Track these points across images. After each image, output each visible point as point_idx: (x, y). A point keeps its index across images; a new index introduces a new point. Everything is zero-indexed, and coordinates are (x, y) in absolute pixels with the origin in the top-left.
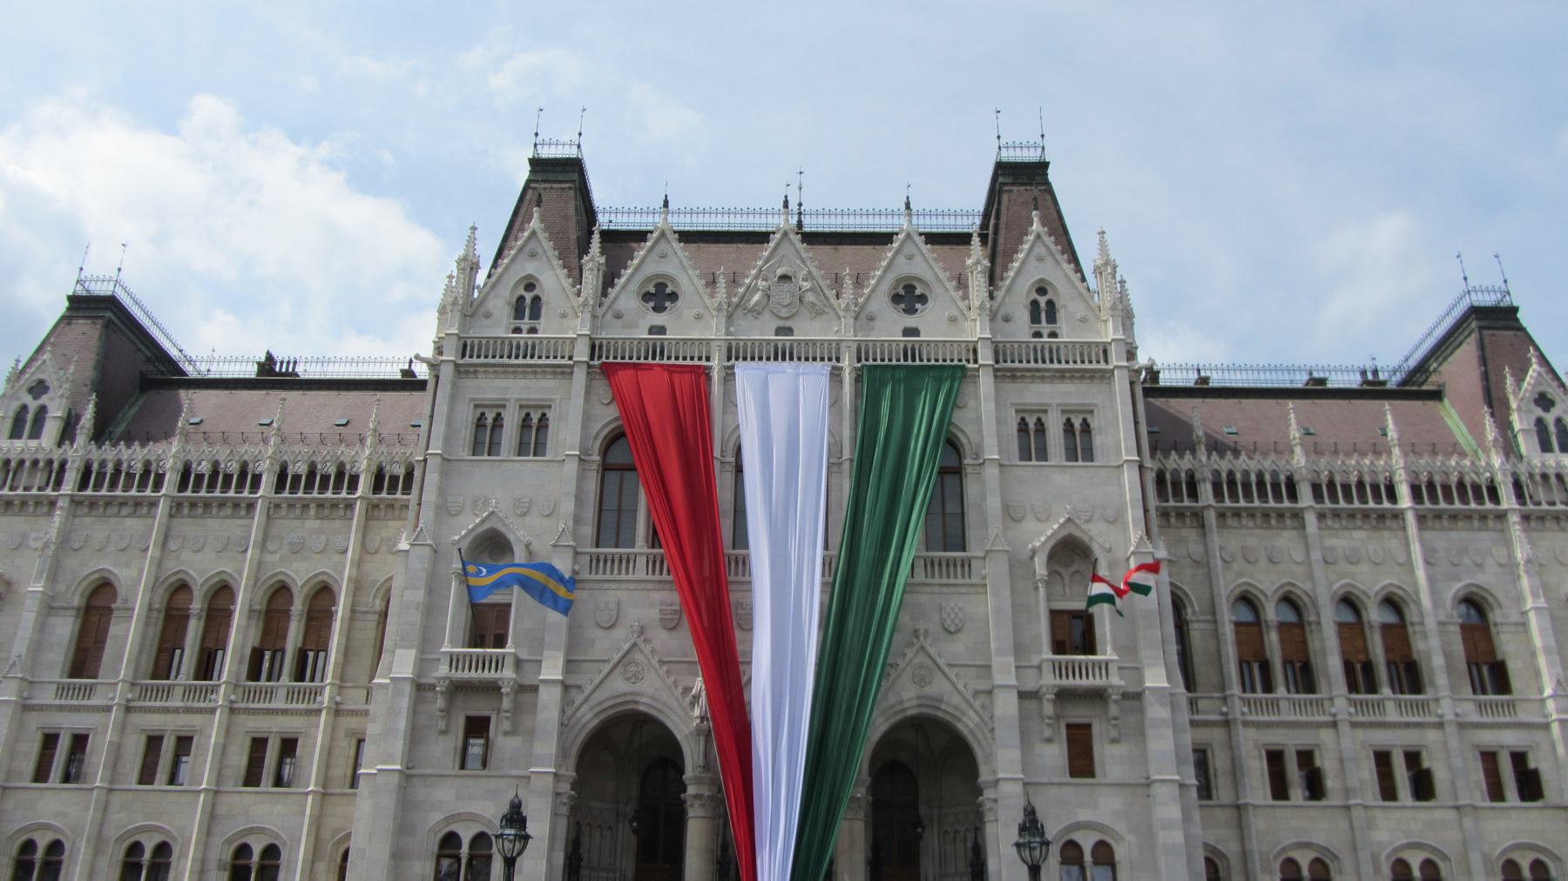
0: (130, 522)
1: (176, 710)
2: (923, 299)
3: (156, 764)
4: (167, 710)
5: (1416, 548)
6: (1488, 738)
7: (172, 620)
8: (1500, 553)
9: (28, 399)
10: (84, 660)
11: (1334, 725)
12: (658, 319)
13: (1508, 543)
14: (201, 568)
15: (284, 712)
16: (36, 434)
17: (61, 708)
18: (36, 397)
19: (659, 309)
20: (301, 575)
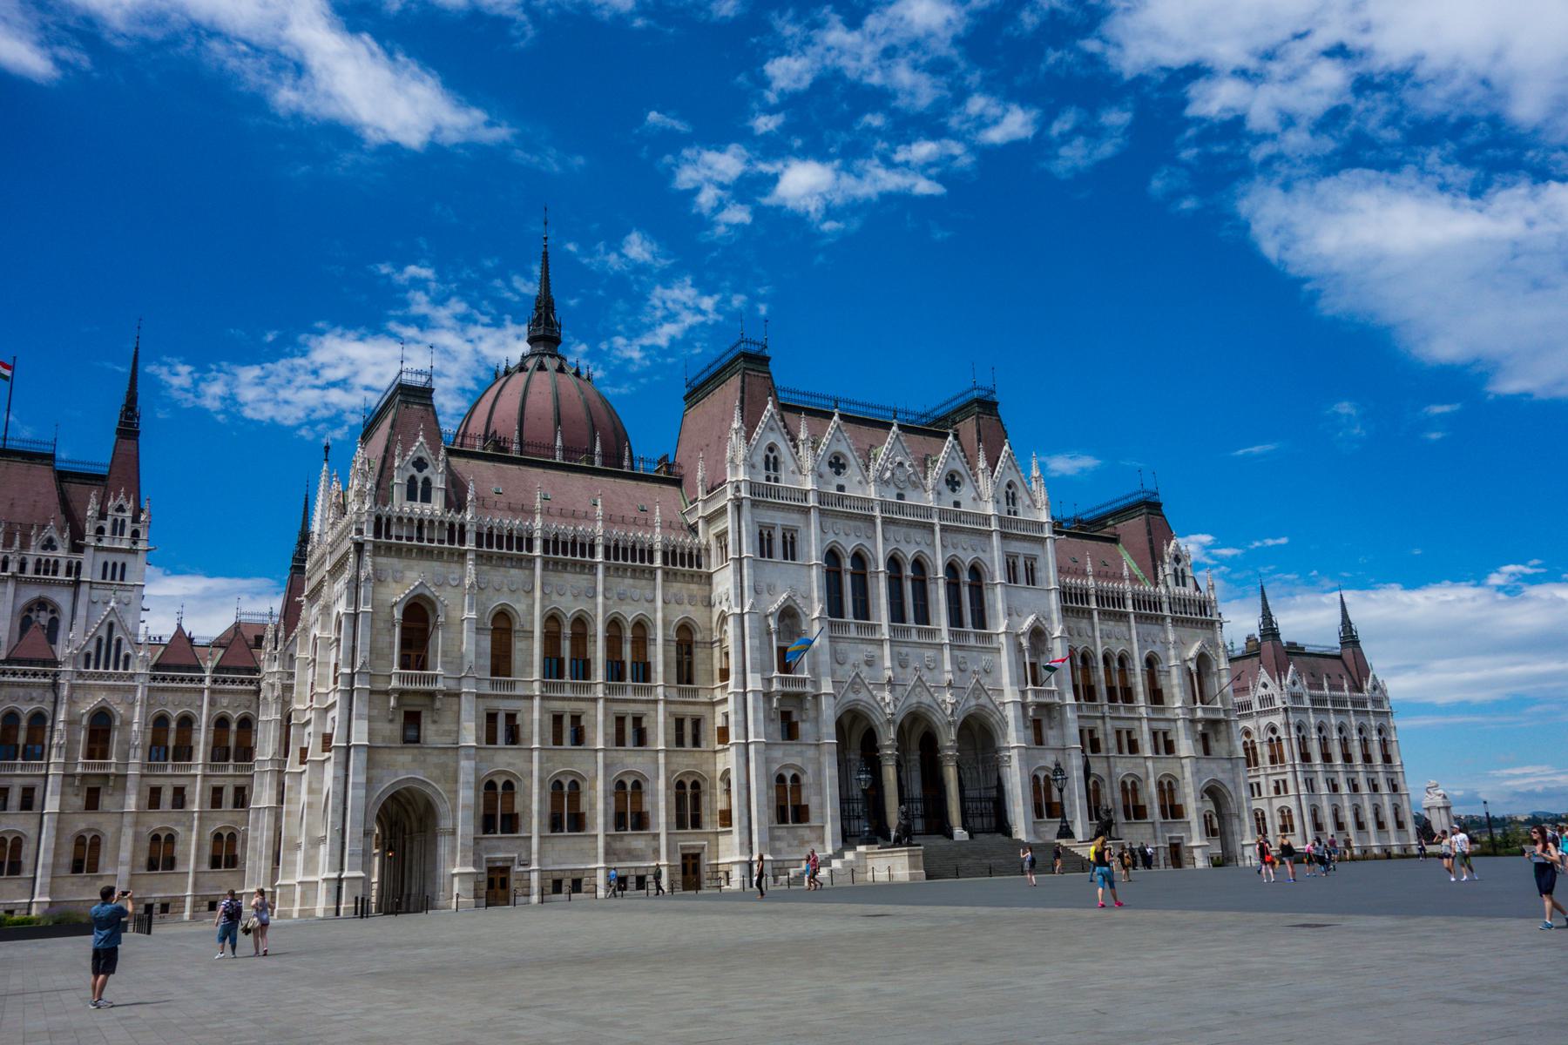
0: (513, 571)
1: (569, 699)
2: (958, 484)
3: (495, 728)
4: (564, 699)
5: (1134, 632)
6: (1156, 725)
7: (551, 639)
8: (1162, 635)
9: (414, 471)
10: (501, 663)
11: (1103, 718)
12: (840, 480)
13: (1165, 632)
14: (569, 607)
15: (634, 701)
16: (426, 498)
17: (496, 696)
18: (420, 470)
19: (838, 473)
20: (630, 613)
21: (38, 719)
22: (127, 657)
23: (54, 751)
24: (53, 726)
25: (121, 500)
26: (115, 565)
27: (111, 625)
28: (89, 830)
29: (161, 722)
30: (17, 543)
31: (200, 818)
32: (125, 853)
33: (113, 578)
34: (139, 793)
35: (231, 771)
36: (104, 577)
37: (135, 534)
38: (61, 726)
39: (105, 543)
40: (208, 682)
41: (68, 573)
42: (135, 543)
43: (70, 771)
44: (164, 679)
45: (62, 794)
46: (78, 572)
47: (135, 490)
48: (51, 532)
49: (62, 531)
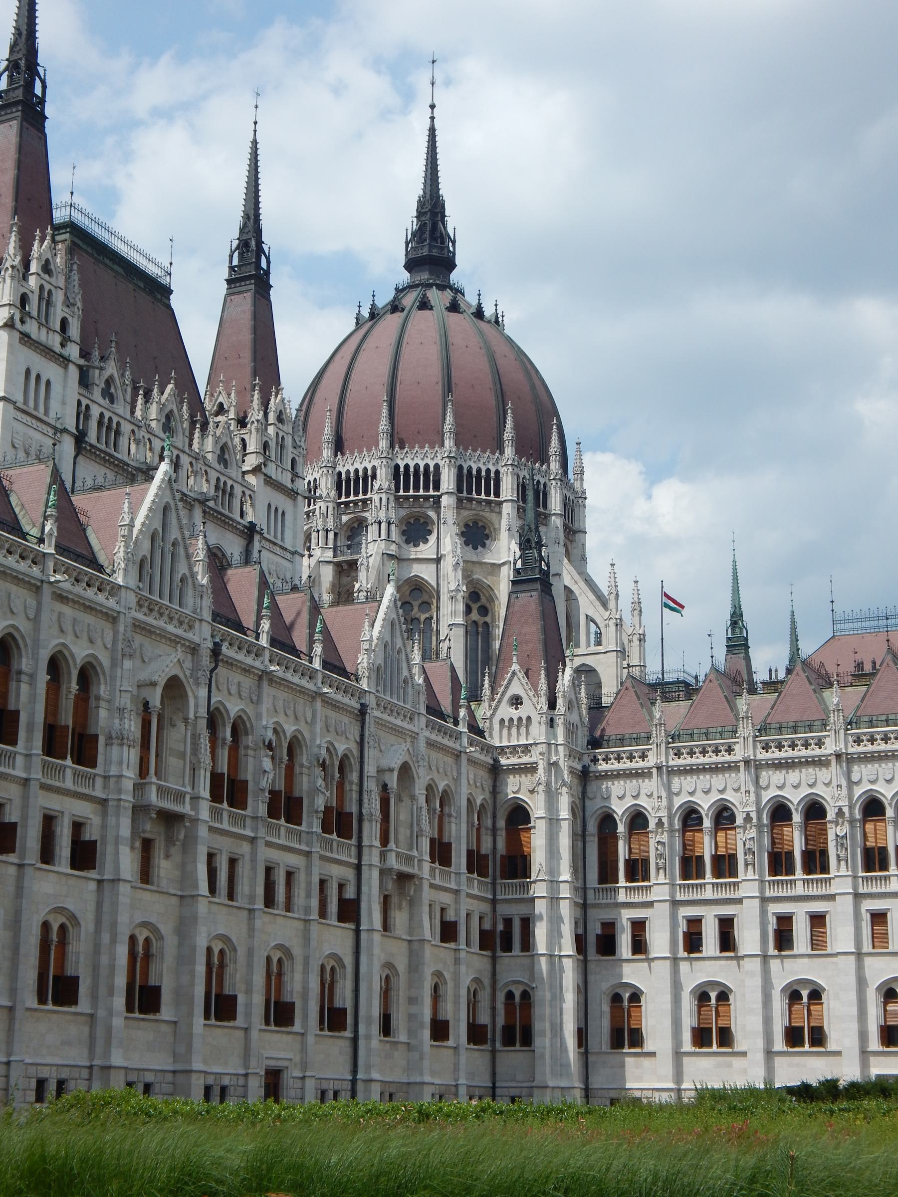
26: (276, 509)
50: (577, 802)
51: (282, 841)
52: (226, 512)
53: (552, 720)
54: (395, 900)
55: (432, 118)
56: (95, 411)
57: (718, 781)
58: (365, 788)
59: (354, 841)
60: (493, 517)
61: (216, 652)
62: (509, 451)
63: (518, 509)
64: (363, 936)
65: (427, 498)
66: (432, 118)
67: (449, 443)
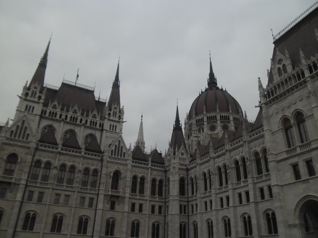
21: (96, 171)
22: (124, 153)
23: (101, 185)
24: (101, 176)
25: (116, 106)
26: (113, 126)
27: (119, 141)
28: (111, 218)
29: (135, 178)
30: (85, 114)
31: (149, 217)
32: (124, 229)
33: (113, 130)
34: (129, 205)
35: (157, 199)
36: (110, 129)
37: (120, 116)
38: (103, 176)
39: (111, 118)
40: (150, 165)
41: (100, 127)
42: (119, 119)
43: (107, 194)
44: (136, 163)
45: (104, 202)
46: (103, 127)
47: (119, 103)
48: (95, 112)
49: (98, 113)
50: (186, 177)
51: (64, 188)
52: (94, 127)
53: (174, 158)
54: (116, 203)
55: (210, 60)
56: (48, 111)
57: (207, 164)
58: (102, 176)
59: (97, 188)
60: (216, 124)
61: (37, 149)
62: (218, 111)
63: (221, 121)
64: (97, 211)
65: (202, 124)
66: (210, 60)
67: (205, 112)
